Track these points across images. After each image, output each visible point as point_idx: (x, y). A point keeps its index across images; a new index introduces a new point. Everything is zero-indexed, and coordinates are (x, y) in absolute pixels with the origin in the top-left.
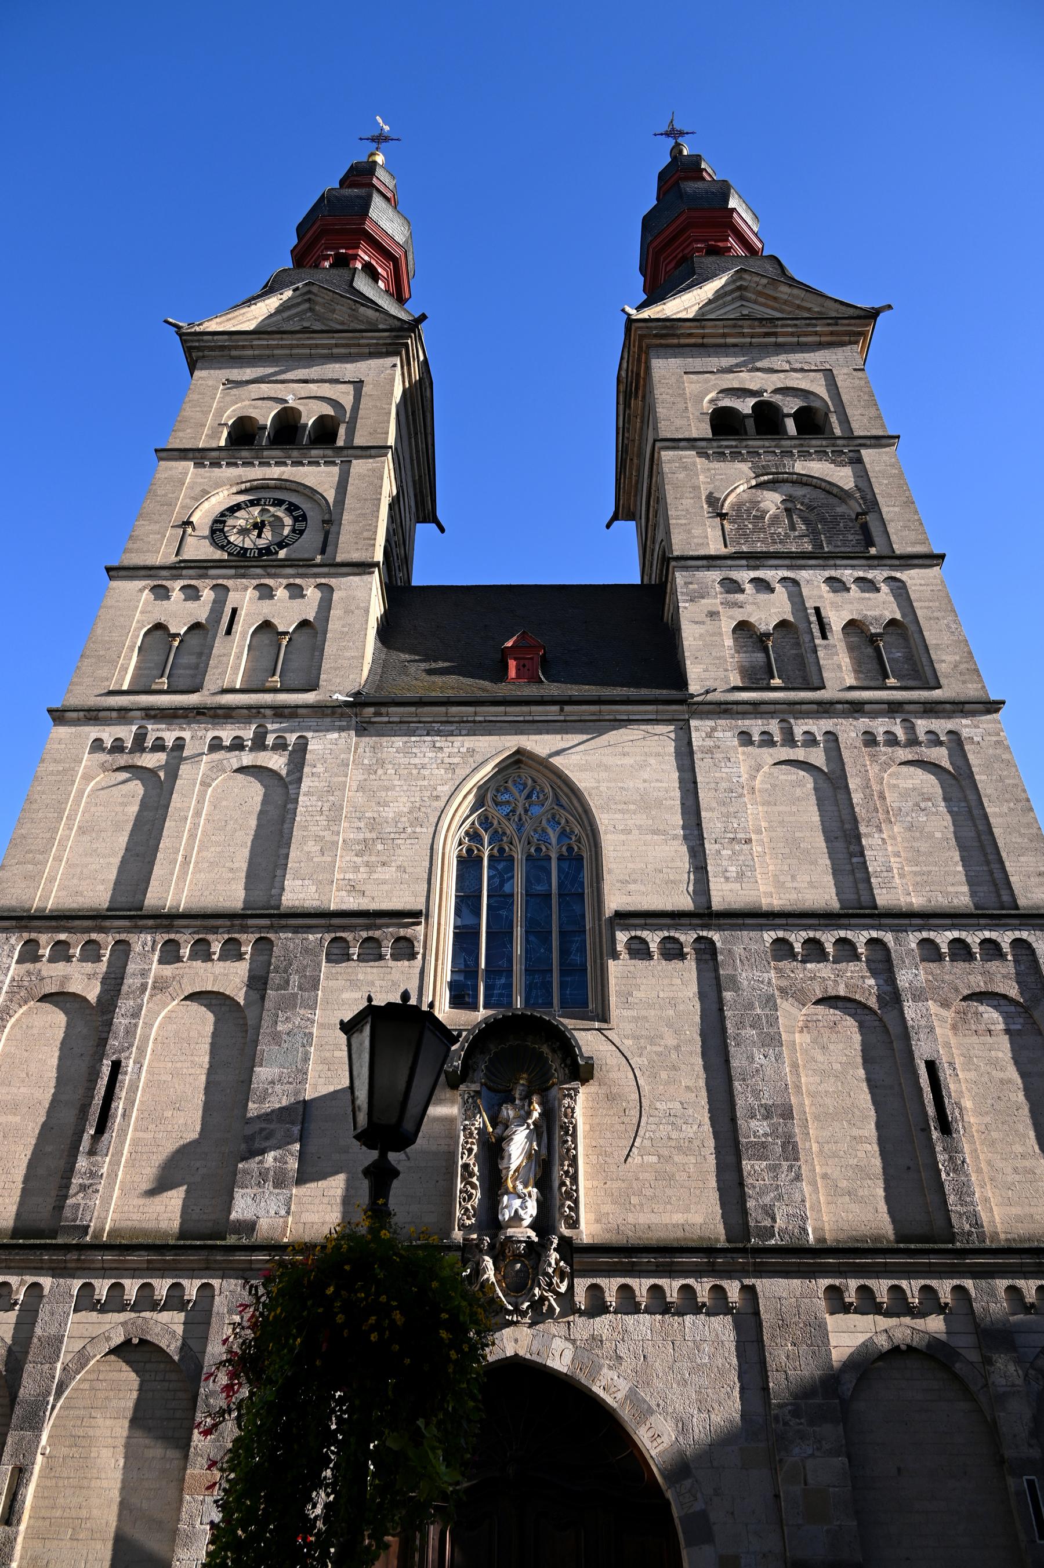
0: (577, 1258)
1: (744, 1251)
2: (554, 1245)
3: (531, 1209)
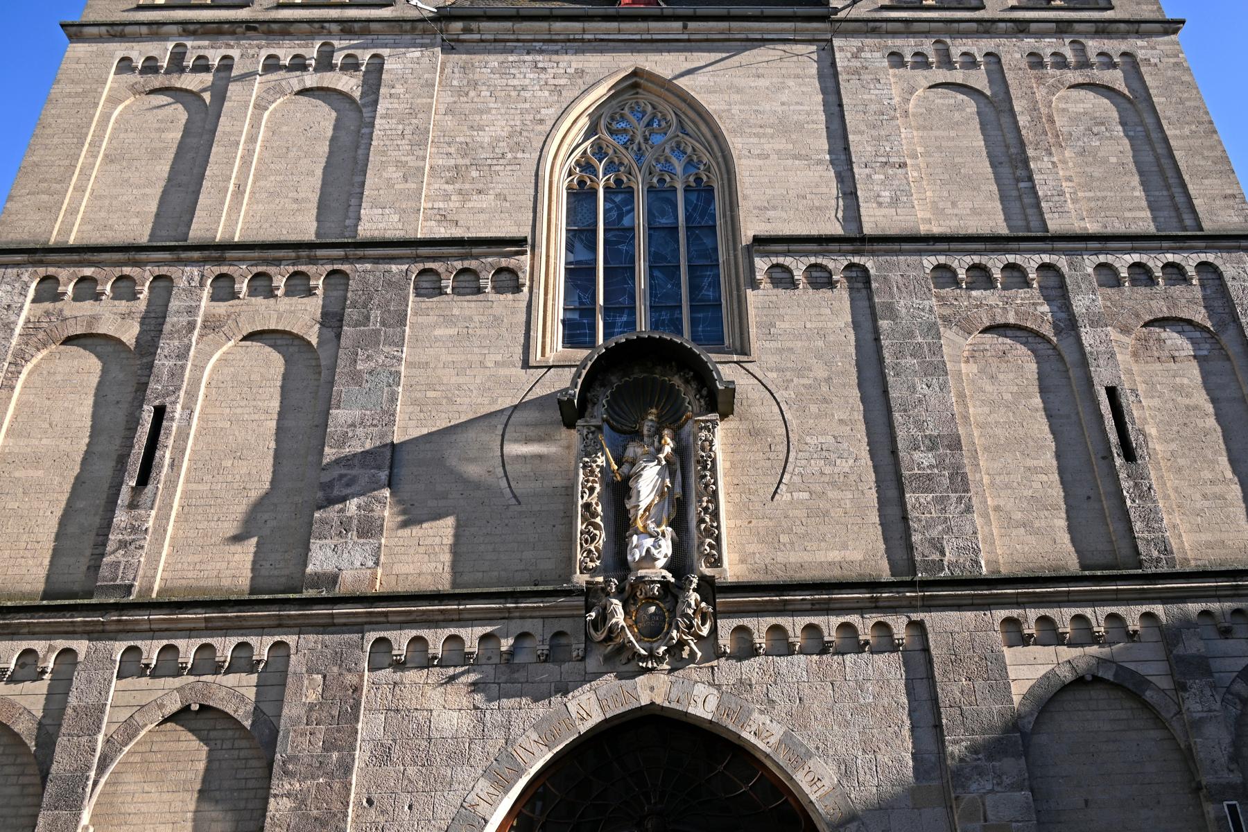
3: (666, 548)
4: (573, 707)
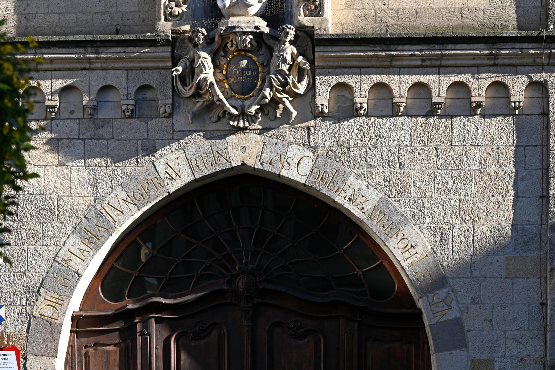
0: (320, 52)
1: (538, 39)
2: (290, 37)
4: (161, 166)
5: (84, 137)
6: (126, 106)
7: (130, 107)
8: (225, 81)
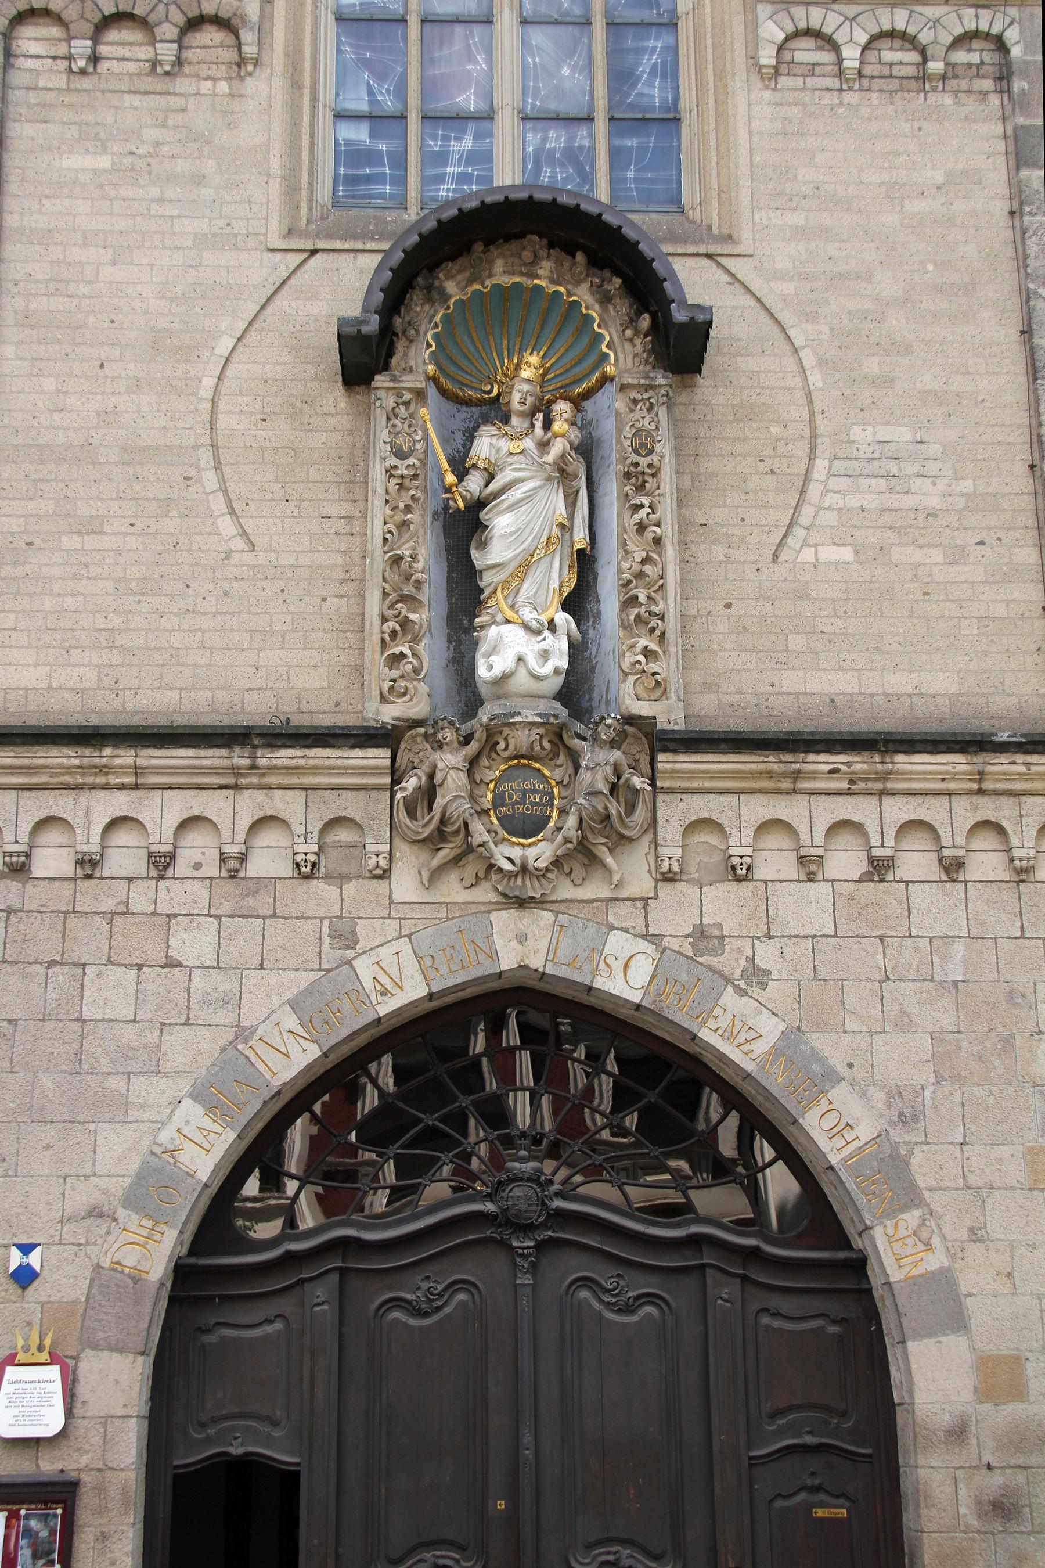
5: (219, 912)
6: (303, 856)
7: (312, 858)
8: (492, 812)
